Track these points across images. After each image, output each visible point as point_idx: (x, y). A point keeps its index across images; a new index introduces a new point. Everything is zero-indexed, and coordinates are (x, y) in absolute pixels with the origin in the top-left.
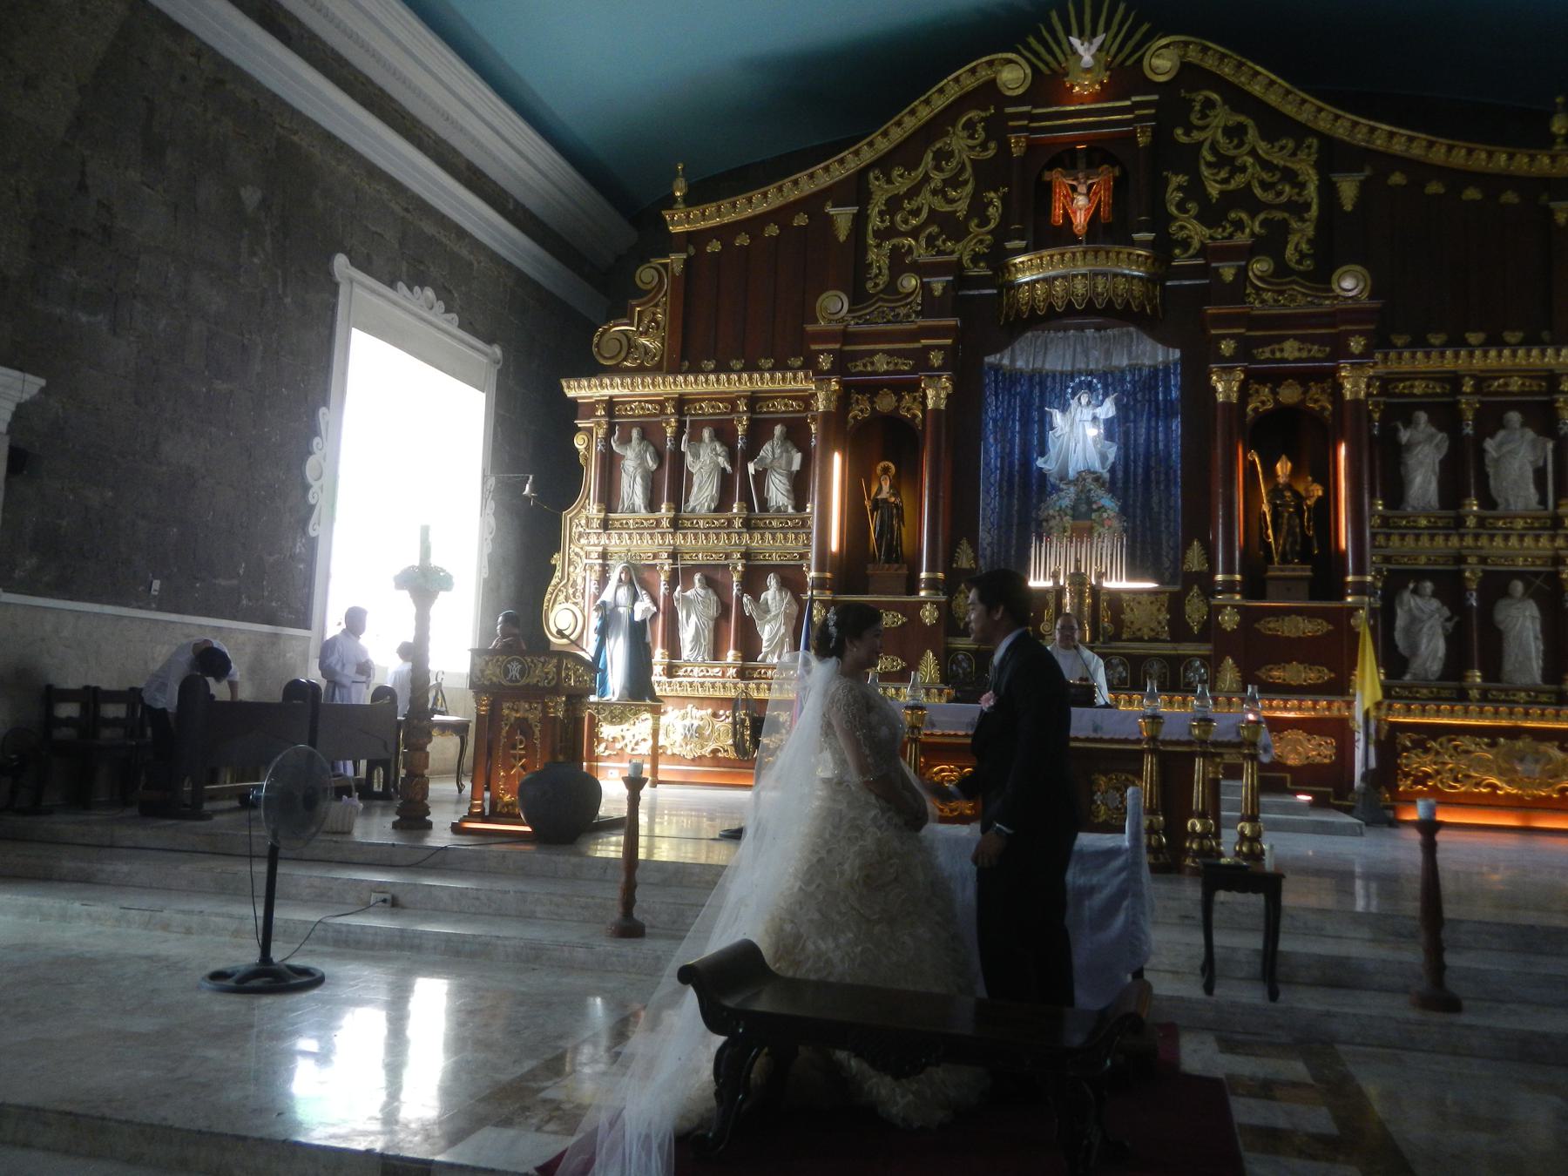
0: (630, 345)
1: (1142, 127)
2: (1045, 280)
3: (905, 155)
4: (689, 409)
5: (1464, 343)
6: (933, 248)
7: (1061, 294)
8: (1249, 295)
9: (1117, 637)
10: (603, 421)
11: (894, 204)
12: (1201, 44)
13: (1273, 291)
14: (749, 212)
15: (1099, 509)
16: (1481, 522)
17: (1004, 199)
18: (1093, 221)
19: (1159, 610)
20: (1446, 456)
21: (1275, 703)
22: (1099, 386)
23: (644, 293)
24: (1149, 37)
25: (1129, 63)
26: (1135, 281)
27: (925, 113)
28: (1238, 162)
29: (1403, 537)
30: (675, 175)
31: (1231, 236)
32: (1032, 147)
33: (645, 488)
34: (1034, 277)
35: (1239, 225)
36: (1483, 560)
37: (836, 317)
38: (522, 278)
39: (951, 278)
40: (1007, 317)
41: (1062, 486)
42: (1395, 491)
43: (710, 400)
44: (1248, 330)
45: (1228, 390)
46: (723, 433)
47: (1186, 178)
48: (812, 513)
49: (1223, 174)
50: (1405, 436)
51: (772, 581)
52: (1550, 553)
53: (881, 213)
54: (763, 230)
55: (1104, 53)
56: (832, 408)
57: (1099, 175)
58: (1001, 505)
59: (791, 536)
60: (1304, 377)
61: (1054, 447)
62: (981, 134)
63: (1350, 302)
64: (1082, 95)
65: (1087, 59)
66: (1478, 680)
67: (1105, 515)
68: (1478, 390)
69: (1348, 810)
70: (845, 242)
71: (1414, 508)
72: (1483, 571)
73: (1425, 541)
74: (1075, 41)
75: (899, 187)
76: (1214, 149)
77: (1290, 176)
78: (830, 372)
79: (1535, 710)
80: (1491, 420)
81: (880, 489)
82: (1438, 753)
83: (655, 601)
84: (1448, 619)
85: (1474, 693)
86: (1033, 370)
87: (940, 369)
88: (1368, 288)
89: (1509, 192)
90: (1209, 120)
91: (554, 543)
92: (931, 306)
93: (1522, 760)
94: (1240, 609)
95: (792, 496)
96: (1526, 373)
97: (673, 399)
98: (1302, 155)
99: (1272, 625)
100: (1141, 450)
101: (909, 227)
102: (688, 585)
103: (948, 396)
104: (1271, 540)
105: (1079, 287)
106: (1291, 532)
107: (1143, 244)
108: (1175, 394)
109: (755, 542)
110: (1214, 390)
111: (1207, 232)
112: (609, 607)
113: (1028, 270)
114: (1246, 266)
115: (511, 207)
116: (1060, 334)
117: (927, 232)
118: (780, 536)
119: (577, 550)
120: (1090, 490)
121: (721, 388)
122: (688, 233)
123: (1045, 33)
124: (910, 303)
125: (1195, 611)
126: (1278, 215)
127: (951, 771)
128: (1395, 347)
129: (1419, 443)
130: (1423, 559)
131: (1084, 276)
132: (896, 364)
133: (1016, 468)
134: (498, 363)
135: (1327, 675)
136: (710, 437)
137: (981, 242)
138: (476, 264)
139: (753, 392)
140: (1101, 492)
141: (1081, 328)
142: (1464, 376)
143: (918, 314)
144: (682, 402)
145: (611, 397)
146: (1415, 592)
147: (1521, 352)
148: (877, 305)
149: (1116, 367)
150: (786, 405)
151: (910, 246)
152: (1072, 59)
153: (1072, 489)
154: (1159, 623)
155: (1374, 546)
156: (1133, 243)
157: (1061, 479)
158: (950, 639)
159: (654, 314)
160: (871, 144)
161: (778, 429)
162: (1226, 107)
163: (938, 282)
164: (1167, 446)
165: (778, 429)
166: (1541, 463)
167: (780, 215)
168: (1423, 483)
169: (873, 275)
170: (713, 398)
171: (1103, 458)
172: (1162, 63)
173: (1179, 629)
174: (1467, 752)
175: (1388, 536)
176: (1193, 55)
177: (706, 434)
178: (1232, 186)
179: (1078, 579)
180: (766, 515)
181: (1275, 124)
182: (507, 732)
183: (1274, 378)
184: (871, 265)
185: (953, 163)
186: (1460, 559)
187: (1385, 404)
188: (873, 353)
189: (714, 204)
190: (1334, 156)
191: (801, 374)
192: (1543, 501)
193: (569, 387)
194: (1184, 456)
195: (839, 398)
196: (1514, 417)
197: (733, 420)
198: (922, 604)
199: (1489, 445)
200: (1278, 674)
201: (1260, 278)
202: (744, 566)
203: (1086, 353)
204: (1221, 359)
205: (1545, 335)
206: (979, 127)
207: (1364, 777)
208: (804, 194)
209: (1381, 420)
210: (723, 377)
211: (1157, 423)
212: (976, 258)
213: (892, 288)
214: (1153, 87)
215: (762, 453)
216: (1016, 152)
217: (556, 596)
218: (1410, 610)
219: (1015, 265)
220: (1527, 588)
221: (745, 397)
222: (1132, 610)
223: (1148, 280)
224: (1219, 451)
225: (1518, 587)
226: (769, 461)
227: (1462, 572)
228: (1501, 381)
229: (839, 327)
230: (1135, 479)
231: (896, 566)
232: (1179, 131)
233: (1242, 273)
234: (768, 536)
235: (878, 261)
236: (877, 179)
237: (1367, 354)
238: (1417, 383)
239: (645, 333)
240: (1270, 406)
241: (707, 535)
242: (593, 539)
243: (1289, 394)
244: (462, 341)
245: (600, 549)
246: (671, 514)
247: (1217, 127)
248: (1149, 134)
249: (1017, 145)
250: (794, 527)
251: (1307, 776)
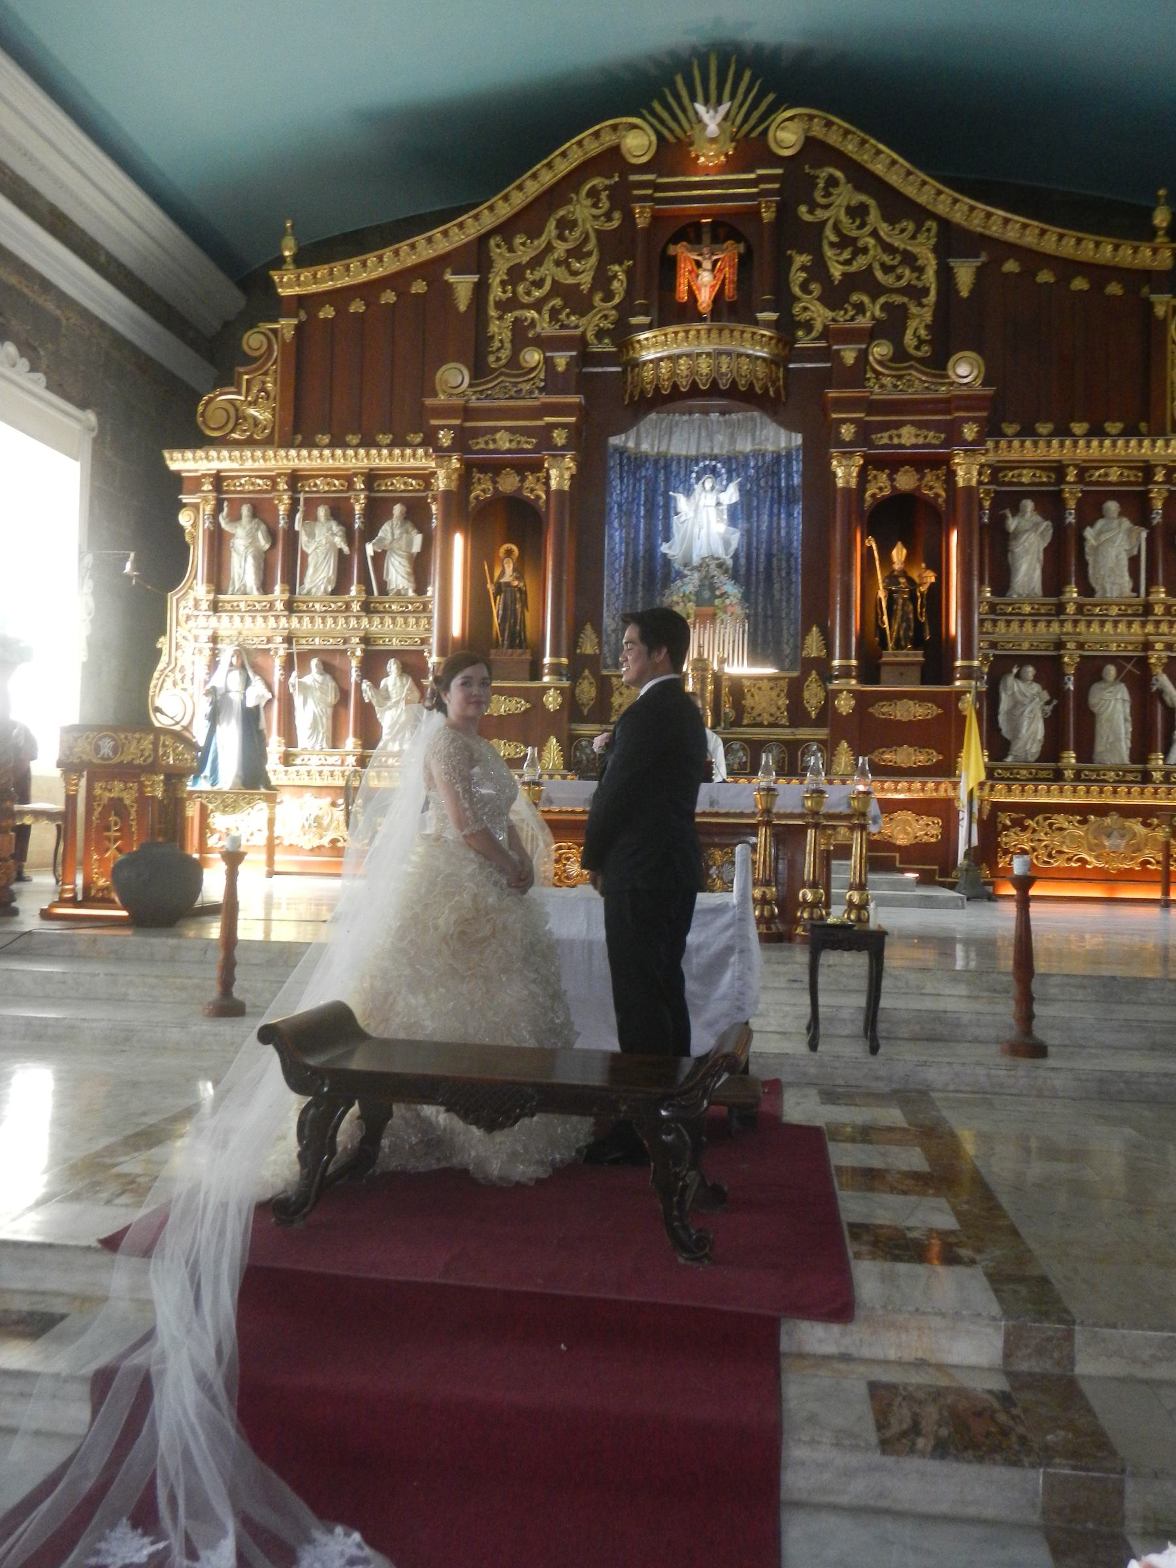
0: (239, 417)
1: (766, 202)
2: (669, 358)
4: (303, 486)
5: (1070, 433)
6: (558, 321)
7: (685, 373)
8: (869, 379)
9: (737, 723)
10: (211, 496)
11: (515, 274)
12: (825, 118)
13: (893, 376)
14: (364, 277)
15: (722, 595)
16: (1080, 608)
17: (629, 273)
18: (718, 299)
19: (778, 695)
20: (1050, 544)
21: (886, 785)
22: (723, 471)
23: (248, 360)
24: (772, 109)
25: (754, 135)
26: (759, 362)
27: (547, 178)
28: (860, 244)
29: (1008, 623)
30: (283, 233)
31: (852, 319)
32: (656, 218)
33: (257, 568)
34: (659, 355)
35: (860, 309)
36: (1081, 646)
37: (457, 391)
38: (119, 340)
39: (574, 353)
40: (631, 396)
41: (686, 572)
42: (1002, 579)
43: (326, 476)
44: (867, 415)
45: (847, 475)
46: (340, 512)
47: (810, 257)
48: (432, 597)
49: (846, 255)
50: (1012, 524)
51: (392, 666)
52: (1141, 639)
53: (503, 283)
54: (378, 298)
55: (729, 123)
56: (453, 486)
57: (723, 251)
58: (625, 590)
59: (412, 621)
60: (921, 463)
61: (679, 532)
62: (605, 204)
63: (964, 388)
64: (707, 166)
65: (712, 128)
66: (1073, 761)
67: (728, 602)
68: (1080, 478)
69: (952, 886)
70: (466, 312)
71: (1020, 595)
72: (1081, 656)
73: (1028, 627)
74: (700, 108)
75: (521, 257)
76: (837, 229)
77: (909, 259)
78: (450, 449)
79: (1123, 789)
80: (1091, 510)
81: (503, 573)
82: (1034, 831)
83: (269, 687)
84: (1048, 703)
85: (1069, 774)
86: (658, 453)
87: (563, 448)
88: (982, 375)
89: (1114, 284)
90: (833, 198)
91: (162, 631)
92: (553, 382)
93: (1109, 836)
94: (857, 695)
95: (412, 579)
96: (1128, 464)
97: (285, 474)
98: (921, 238)
99: (885, 710)
100: (764, 536)
101: (532, 299)
102: (304, 670)
103: (572, 477)
104: (886, 626)
105: (704, 366)
106: (905, 618)
107: (767, 324)
108: (797, 480)
109: (374, 625)
110: (834, 475)
111: (830, 314)
112: (220, 692)
114: (867, 349)
115: (103, 259)
116: (685, 418)
117: (551, 304)
118: (400, 620)
119: (186, 633)
120: (713, 577)
121: (337, 464)
122: (300, 299)
123: (671, 100)
124: (533, 379)
126: (898, 299)
127: (569, 848)
128: (1005, 435)
129: (1027, 531)
130: (1026, 645)
131: (708, 354)
132: (519, 442)
133: (641, 553)
134: (93, 430)
135: (936, 757)
136: (326, 515)
137: (605, 317)
138: (64, 321)
139: (371, 469)
140: (724, 578)
141: (706, 411)
142: (1068, 466)
143: (541, 390)
144: (295, 479)
145: (219, 471)
146: (1018, 676)
147: (1120, 443)
148: (502, 378)
149: (740, 452)
150: (405, 483)
151: (533, 320)
152: (697, 127)
153: (696, 575)
154: (779, 708)
155: (981, 633)
156: (756, 322)
157: (685, 565)
158: (574, 726)
159: (264, 383)
160: (491, 208)
161: (397, 509)
162: (850, 185)
163: (561, 357)
164: (788, 533)
165: (397, 509)
166: (1135, 552)
169: (494, 349)
170: (328, 475)
171: (727, 544)
173: (797, 715)
174: (1061, 829)
175: (995, 622)
176: (818, 131)
177: (322, 512)
178: (854, 268)
180: (385, 598)
182: (100, 813)
183: (891, 463)
184: (492, 337)
185: (577, 233)
186: (1060, 645)
187: (996, 492)
188: (497, 430)
189: (326, 266)
191: (420, 451)
192: (1136, 589)
193: (172, 459)
194: (805, 544)
195: (460, 477)
196: (1112, 506)
197: (349, 498)
198: (544, 690)
199: (1089, 533)
200: (890, 757)
201: (880, 363)
202: (364, 651)
203: (710, 437)
204: (841, 443)
205: (1143, 426)
206: (604, 195)
207: (966, 855)
208: (421, 260)
209: (993, 507)
210: (339, 452)
211: (779, 510)
213: (514, 361)
214: (778, 161)
215: (381, 534)
216: (642, 222)
217: (164, 681)
218: (1013, 693)
219: (639, 341)
220: (1119, 672)
221: (362, 474)
222: (752, 695)
223: (773, 362)
224: (838, 537)
225: (1111, 671)
226: (387, 542)
227: (1061, 657)
228: (1102, 471)
229: (460, 402)
230: (757, 567)
231: (519, 651)
232: (803, 209)
233: (863, 356)
234: (388, 621)
235: (500, 334)
236: (498, 246)
237: (979, 441)
238: (1025, 472)
239: (254, 403)
240: (887, 492)
241: (323, 619)
242: (202, 621)
243: (906, 481)
244: (50, 404)
245: (210, 632)
246: (286, 596)
247: (840, 206)
248: (773, 209)
249: (642, 217)
250: (414, 612)
251: (915, 855)
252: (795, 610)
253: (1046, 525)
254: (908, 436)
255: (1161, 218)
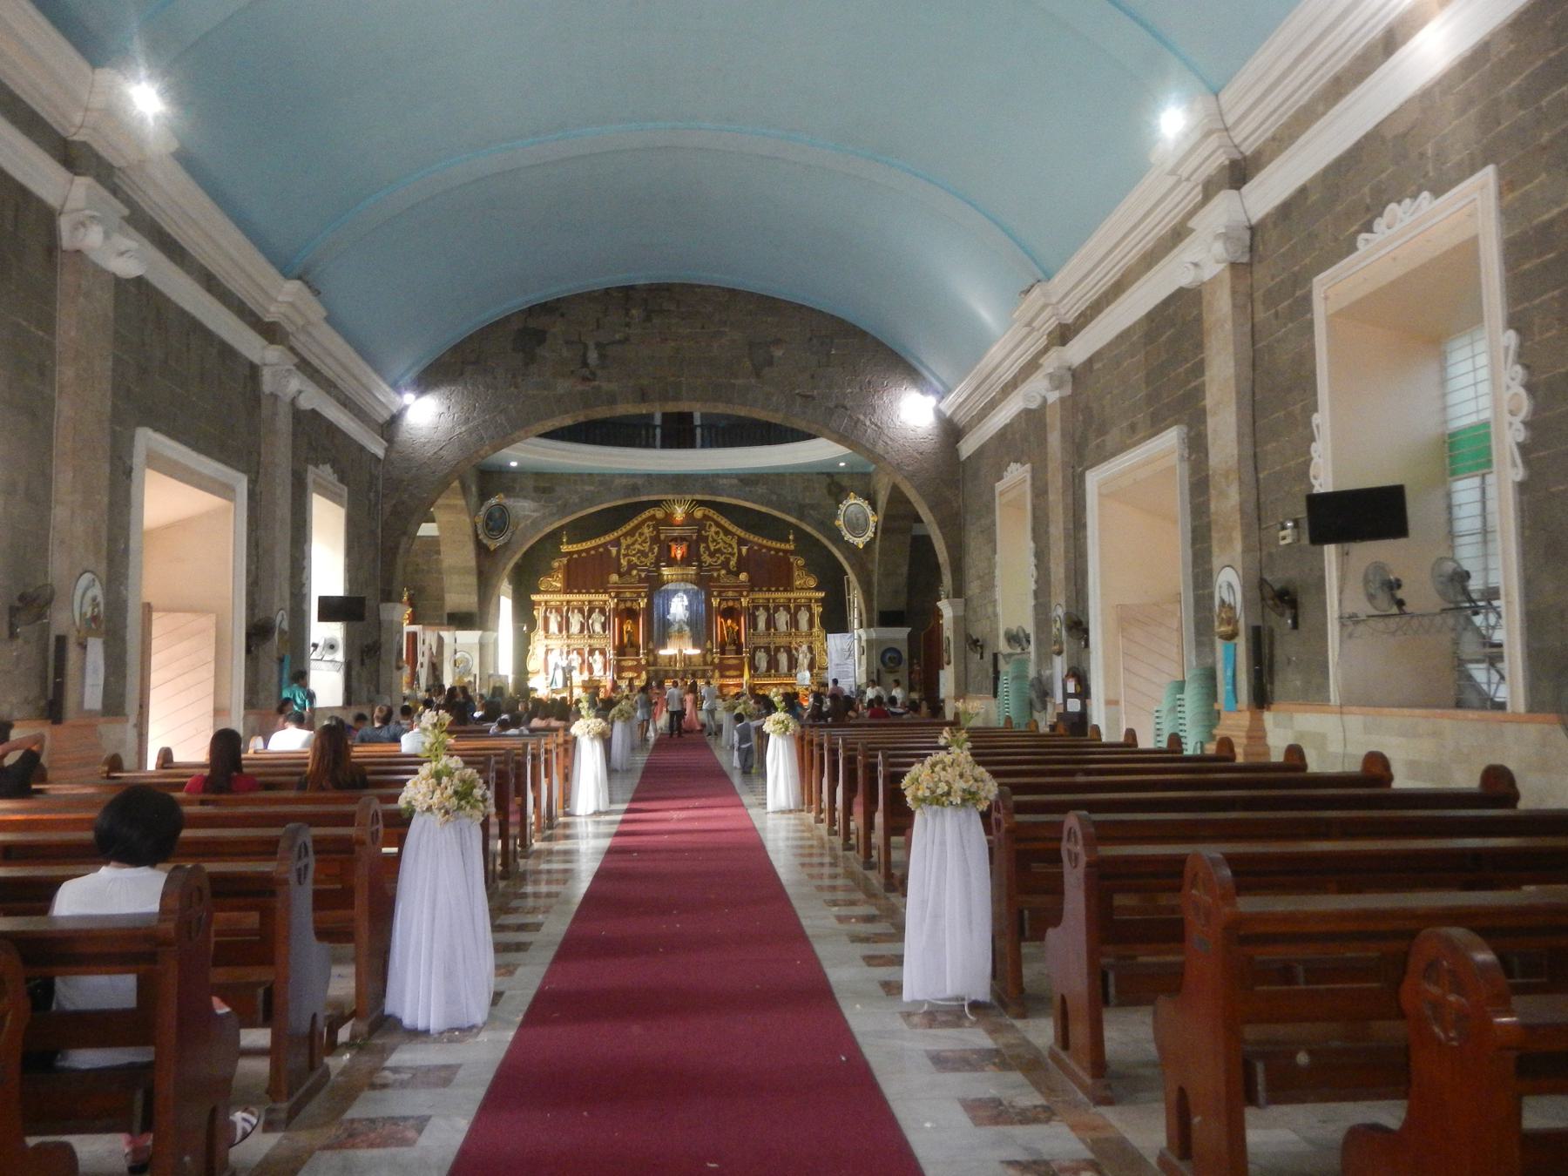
3: (631, 533)
11: (628, 547)
18: (682, 557)
42: (755, 628)
46: (581, 611)
51: (597, 652)
60: (733, 600)
77: (730, 546)
80: (776, 609)
92: (641, 580)
113: (666, 571)
125: (709, 658)
144: (568, 602)
167: (595, 548)
168: (762, 625)
172: (698, 514)
173: (705, 663)
176: (707, 512)
179: (680, 651)
181: (727, 532)
190: (741, 542)
196: (781, 608)
200: (728, 673)
212: (651, 563)
213: (629, 572)
233: (719, 575)
237: (747, 596)
243: (731, 604)
252: (703, 638)
253: (766, 614)
254: (730, 594)
255: (791, 537)
